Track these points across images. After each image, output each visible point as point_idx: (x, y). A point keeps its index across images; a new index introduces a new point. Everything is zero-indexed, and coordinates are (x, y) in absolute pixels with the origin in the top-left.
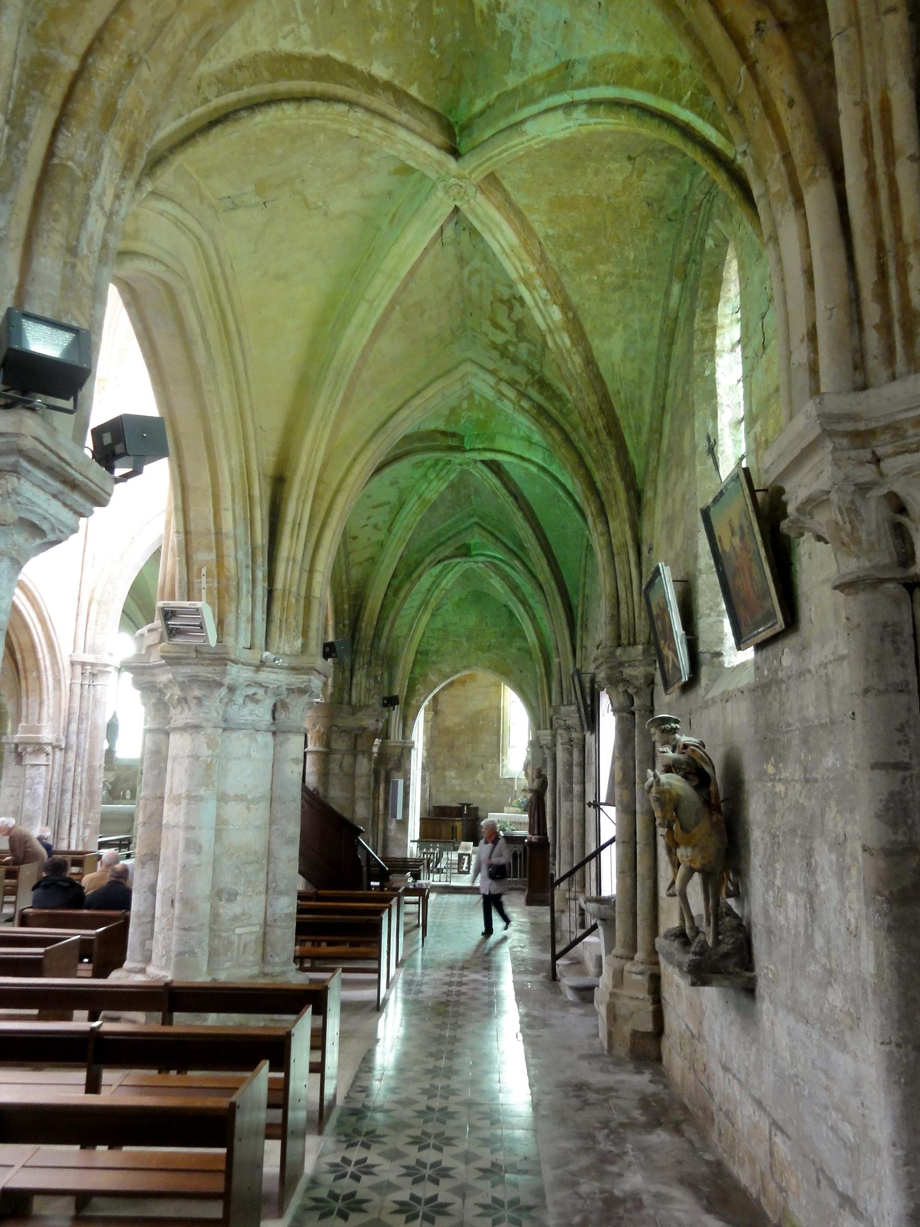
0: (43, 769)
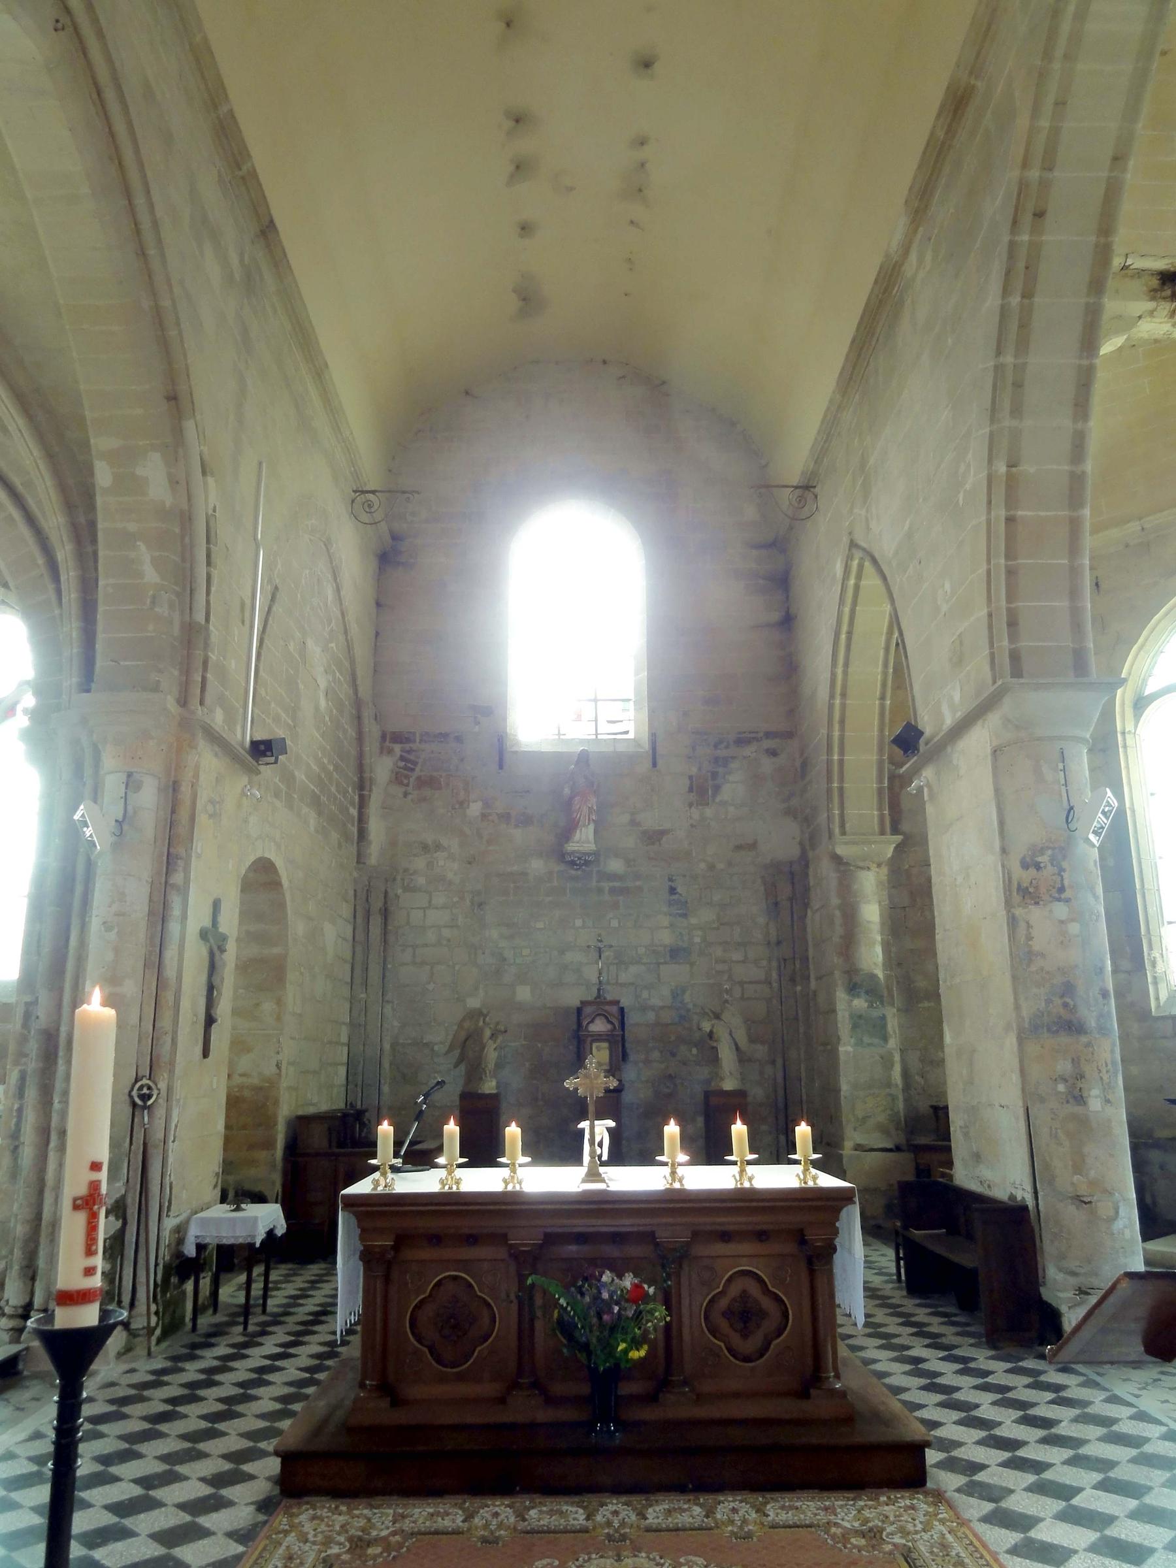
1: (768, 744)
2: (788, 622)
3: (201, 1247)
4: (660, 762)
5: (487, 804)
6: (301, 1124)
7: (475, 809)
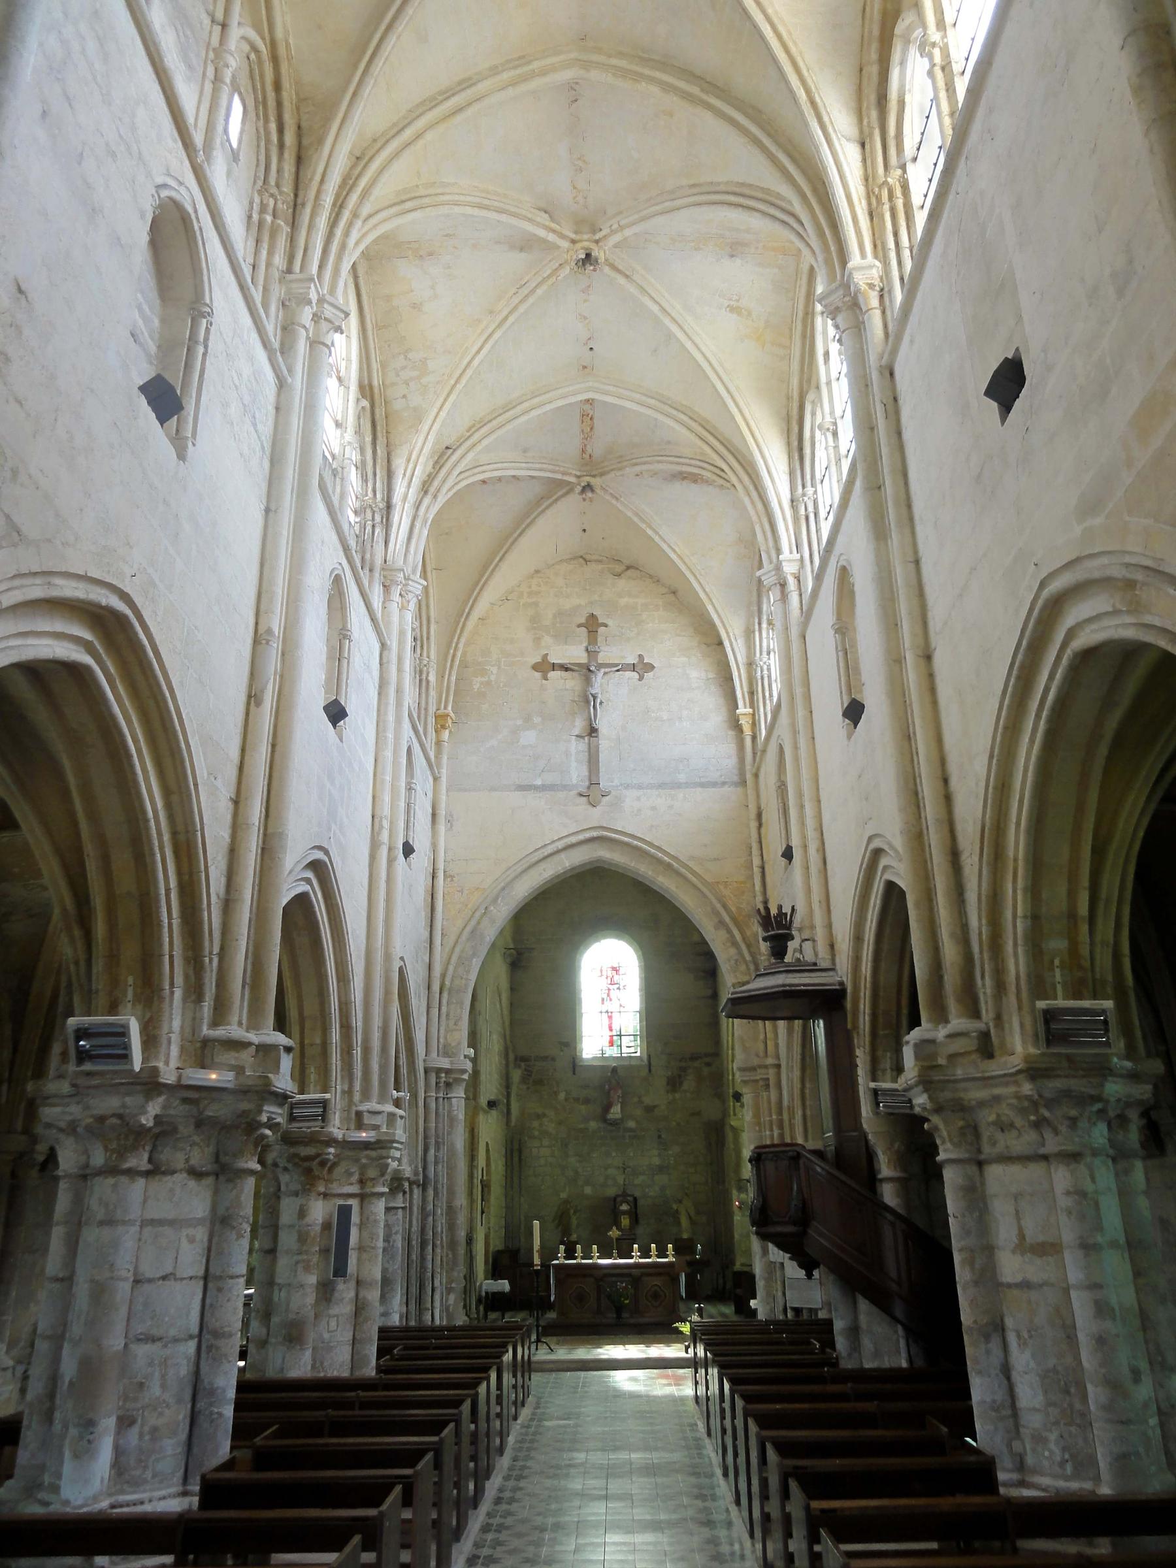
1: (707, 1060)
3: (487, 1293)
4: (653, 1069)
7: (562, 1096)
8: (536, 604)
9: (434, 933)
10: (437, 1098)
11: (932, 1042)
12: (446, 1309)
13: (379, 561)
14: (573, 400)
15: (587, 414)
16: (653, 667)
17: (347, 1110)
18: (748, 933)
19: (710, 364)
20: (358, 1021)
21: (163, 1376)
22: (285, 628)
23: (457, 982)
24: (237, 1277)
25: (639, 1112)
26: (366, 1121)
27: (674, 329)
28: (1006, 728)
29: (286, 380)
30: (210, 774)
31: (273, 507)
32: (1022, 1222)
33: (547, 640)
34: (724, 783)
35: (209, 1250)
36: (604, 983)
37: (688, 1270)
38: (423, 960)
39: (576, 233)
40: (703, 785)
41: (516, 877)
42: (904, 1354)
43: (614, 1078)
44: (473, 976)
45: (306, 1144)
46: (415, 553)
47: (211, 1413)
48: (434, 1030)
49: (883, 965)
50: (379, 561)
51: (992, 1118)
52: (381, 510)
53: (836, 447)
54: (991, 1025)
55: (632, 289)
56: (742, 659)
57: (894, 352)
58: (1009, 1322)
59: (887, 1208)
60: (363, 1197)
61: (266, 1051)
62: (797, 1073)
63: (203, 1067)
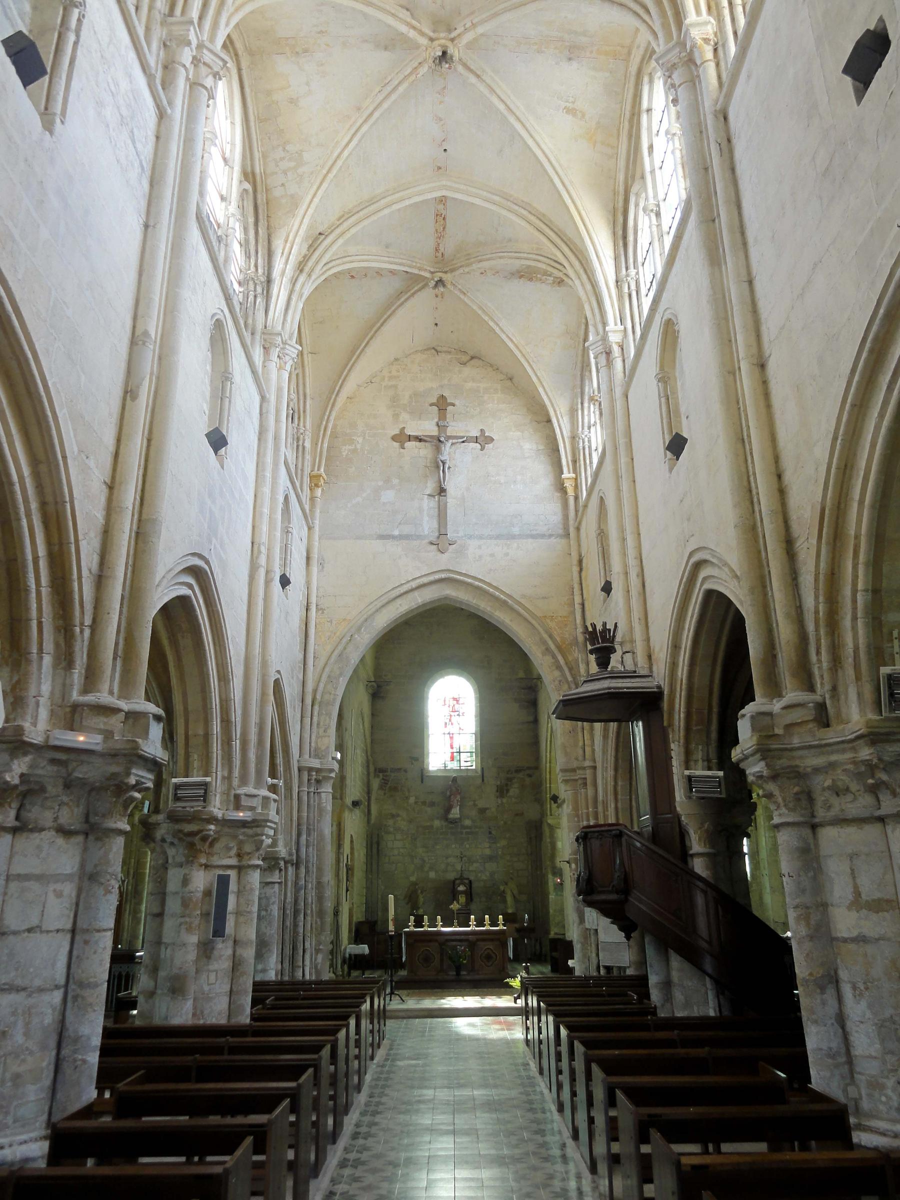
0: (277, 886)
1: (528, 772)
2: (536, 721)
3: (350, 955)
5: (416, 798)
6: (359, 924)
7: (412, 800)
8: (395, 387)
9: (307, 656)
10: (308, 793)
11: (770, 714)
12: (315, 966)
13: (260, 327)
14: (429, 196)
15: (441, 212)
16: (492, 440)
17: (227, 793)
18: (570, 658)
19: (549, 160)
20: (237, 716)
21: (27, 1024)
22: (162, 336)
23: (326, 697)
24: (105, 930)
25: (474, 813)
26: (243, 803)
27: (518, 126)
28: (853, 406)
29: (166, 111)
30: (81, 451)
31: (151, 223)
32: (858, 881)
33: (404, 416)
34: (550, 536)
35: (77, 905)
36: (446, 711)
37: (516, 935)
38: (298, 677)
39: (434, 31)
40: (533, 537)
41: (377, 611)
42: (711, 1004)
43: (454, 785)
44: (340, 692)
45: (189, 822)
46: (292, 322)
47: (75, 1060)
48: (307, 735)
49: (698, 669)
50: (260, 327)
51: (828, 783)
52: (262, 283)
53: (659, 226)
54: (827, 696)
55: (482, 88)
56: (567, 434)
57: (729, 96)
58: (843, 975)
59: (699, 878)
60: (240, 869)
61: (133, 717)
62: (611, 772)
63: (72, 730)
